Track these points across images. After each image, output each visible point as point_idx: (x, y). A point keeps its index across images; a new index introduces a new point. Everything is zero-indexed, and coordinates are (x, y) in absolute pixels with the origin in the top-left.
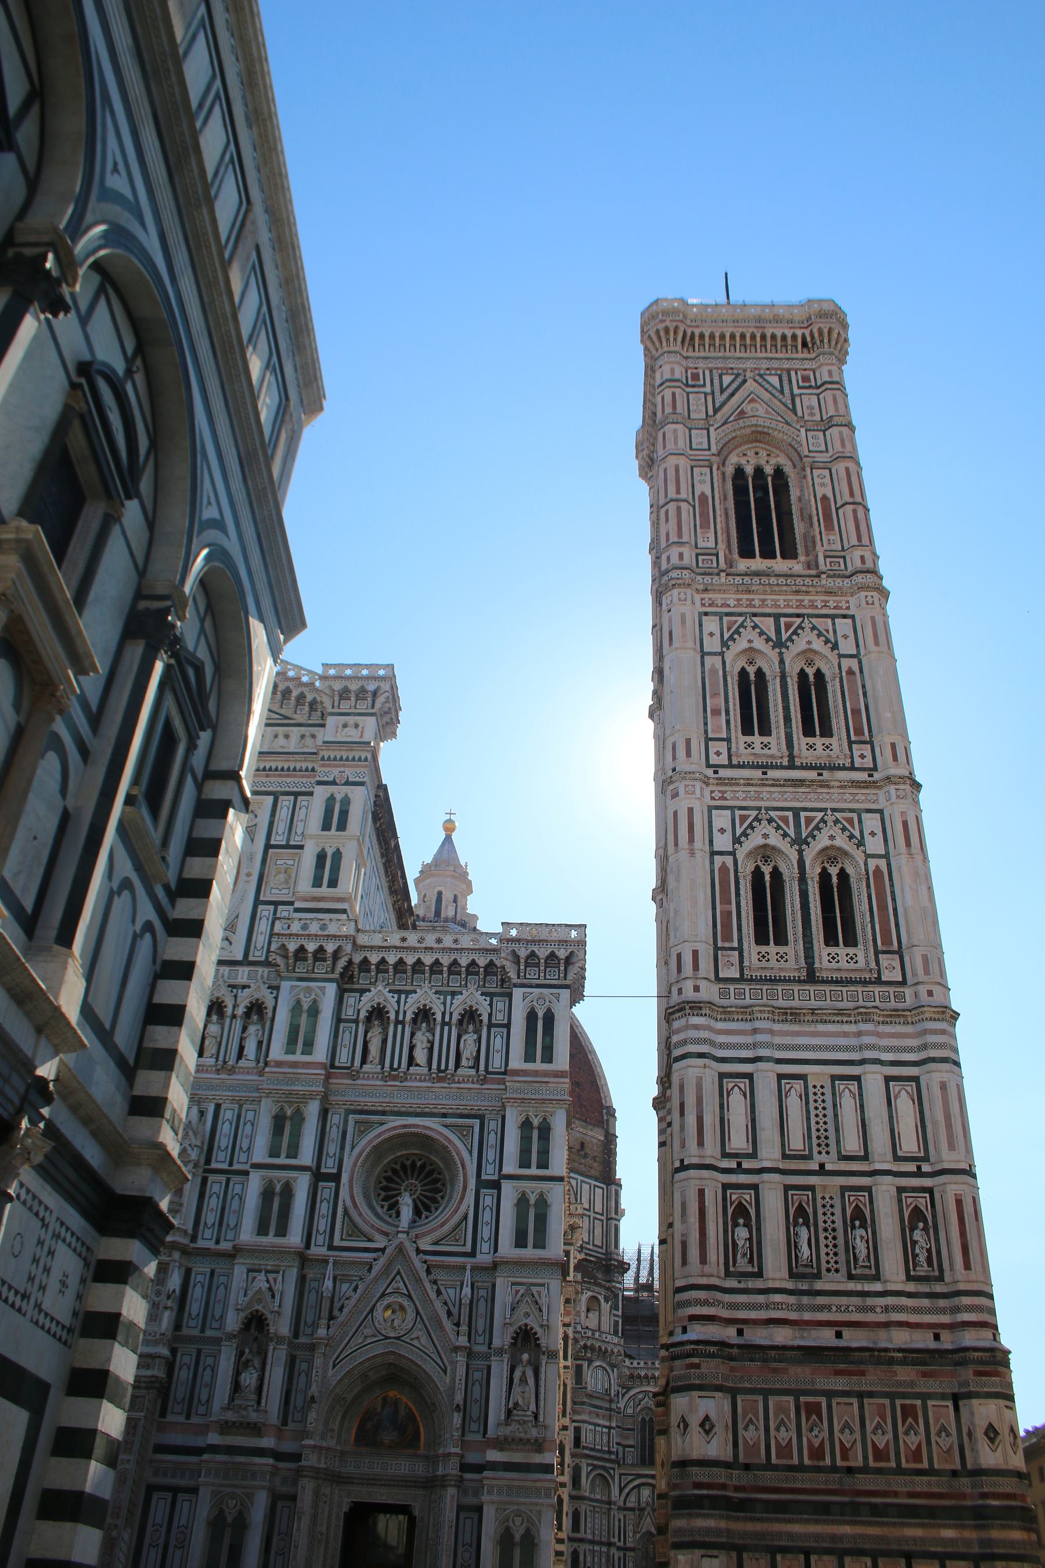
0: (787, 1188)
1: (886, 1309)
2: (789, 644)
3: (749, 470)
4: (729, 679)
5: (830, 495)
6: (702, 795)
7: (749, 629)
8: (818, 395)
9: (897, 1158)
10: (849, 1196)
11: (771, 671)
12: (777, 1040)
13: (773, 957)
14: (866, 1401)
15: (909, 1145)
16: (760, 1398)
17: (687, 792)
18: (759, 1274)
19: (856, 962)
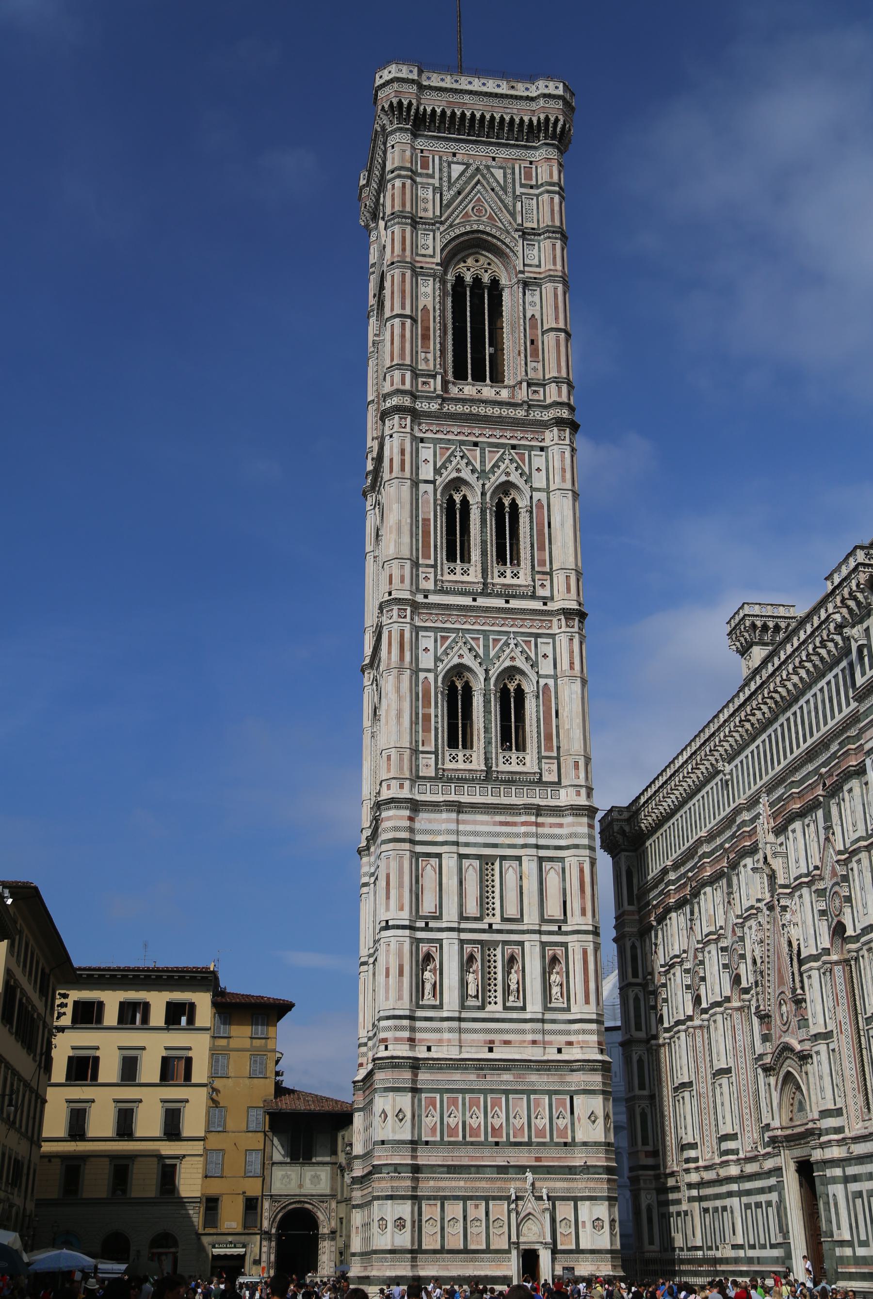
0: (462, 942)
2: (491, 476)
3: (468, 278)
4: (438, 508)
5: (538, 316)
6: (412, 619)
7: (458, 458)
8: (537, 196)
9: (543, 920)
11: (474, 499)
12: (462, 827)
13: (460, 757)
14: (511, 1096)
15: (554, 910)
16: (438, 1096)
17: (400, 616)
18: (440, 1007)
19: (524, 764)
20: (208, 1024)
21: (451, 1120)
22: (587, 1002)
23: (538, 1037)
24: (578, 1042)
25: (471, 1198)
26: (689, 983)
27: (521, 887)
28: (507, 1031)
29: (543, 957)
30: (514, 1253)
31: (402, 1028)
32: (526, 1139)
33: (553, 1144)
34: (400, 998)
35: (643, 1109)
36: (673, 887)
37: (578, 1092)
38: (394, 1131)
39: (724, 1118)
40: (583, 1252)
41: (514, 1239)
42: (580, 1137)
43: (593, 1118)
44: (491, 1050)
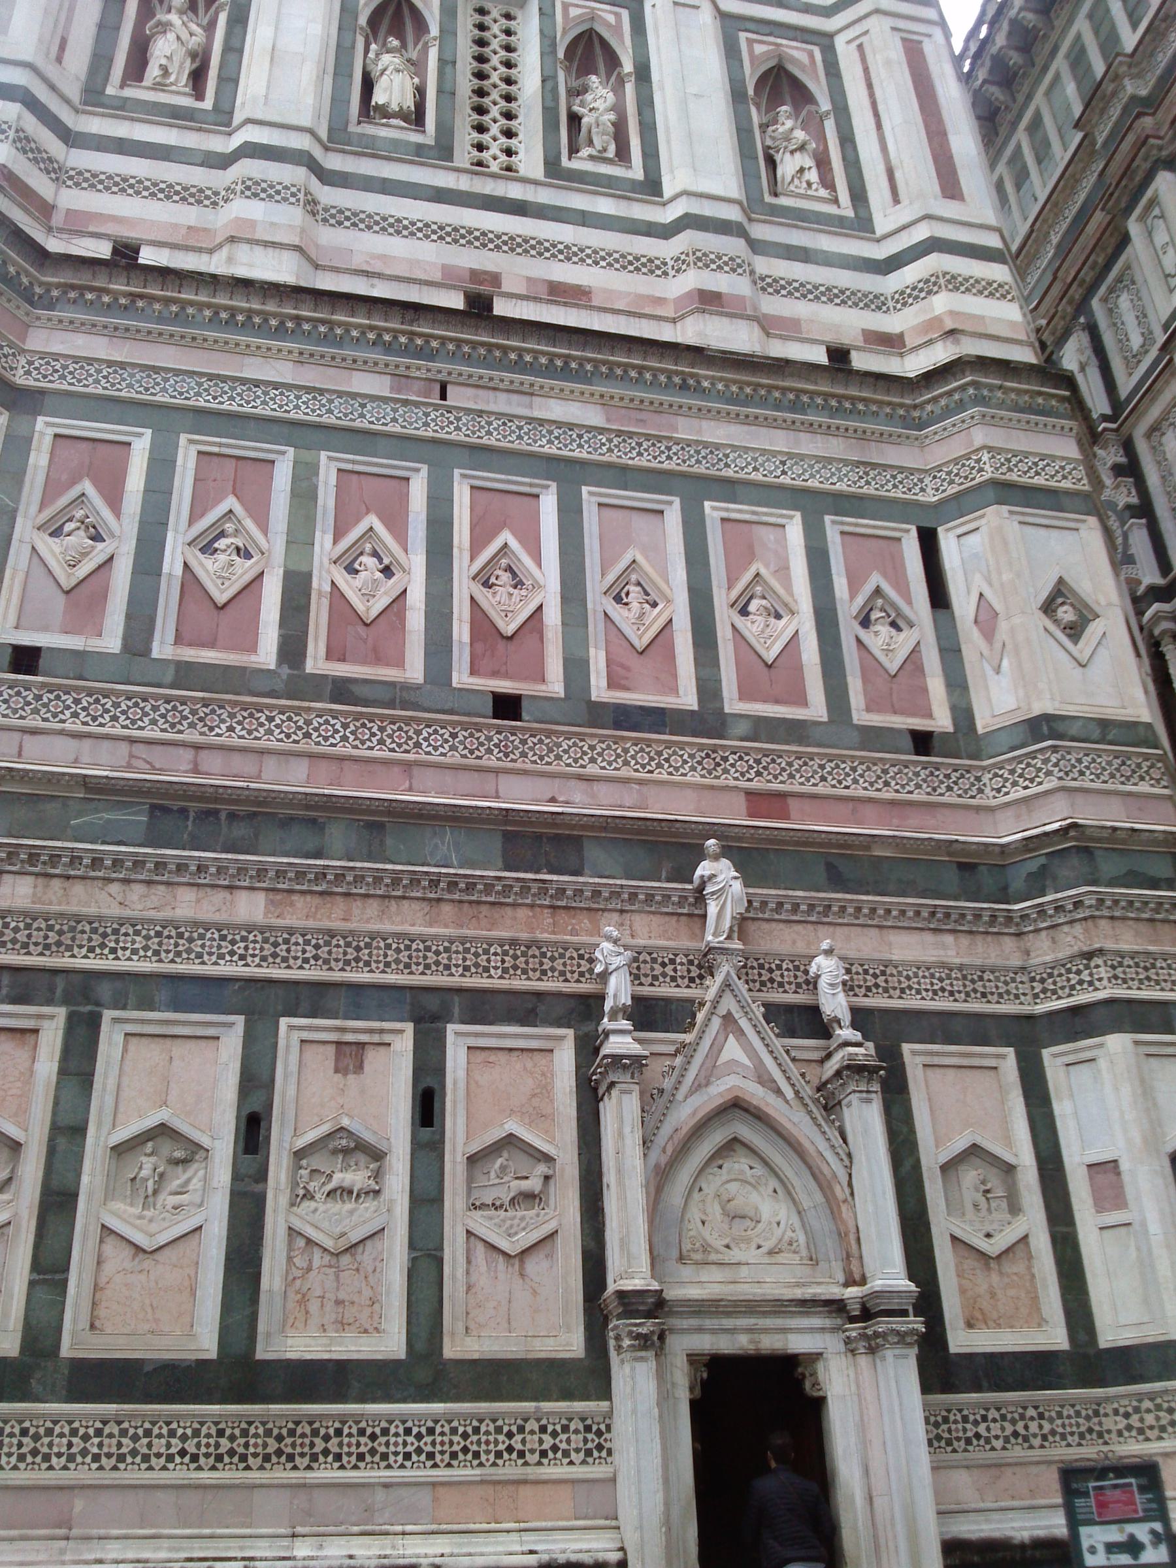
1: (680, 264)
22: (950, 187)
28: (568, 254)
32: (687, 698)
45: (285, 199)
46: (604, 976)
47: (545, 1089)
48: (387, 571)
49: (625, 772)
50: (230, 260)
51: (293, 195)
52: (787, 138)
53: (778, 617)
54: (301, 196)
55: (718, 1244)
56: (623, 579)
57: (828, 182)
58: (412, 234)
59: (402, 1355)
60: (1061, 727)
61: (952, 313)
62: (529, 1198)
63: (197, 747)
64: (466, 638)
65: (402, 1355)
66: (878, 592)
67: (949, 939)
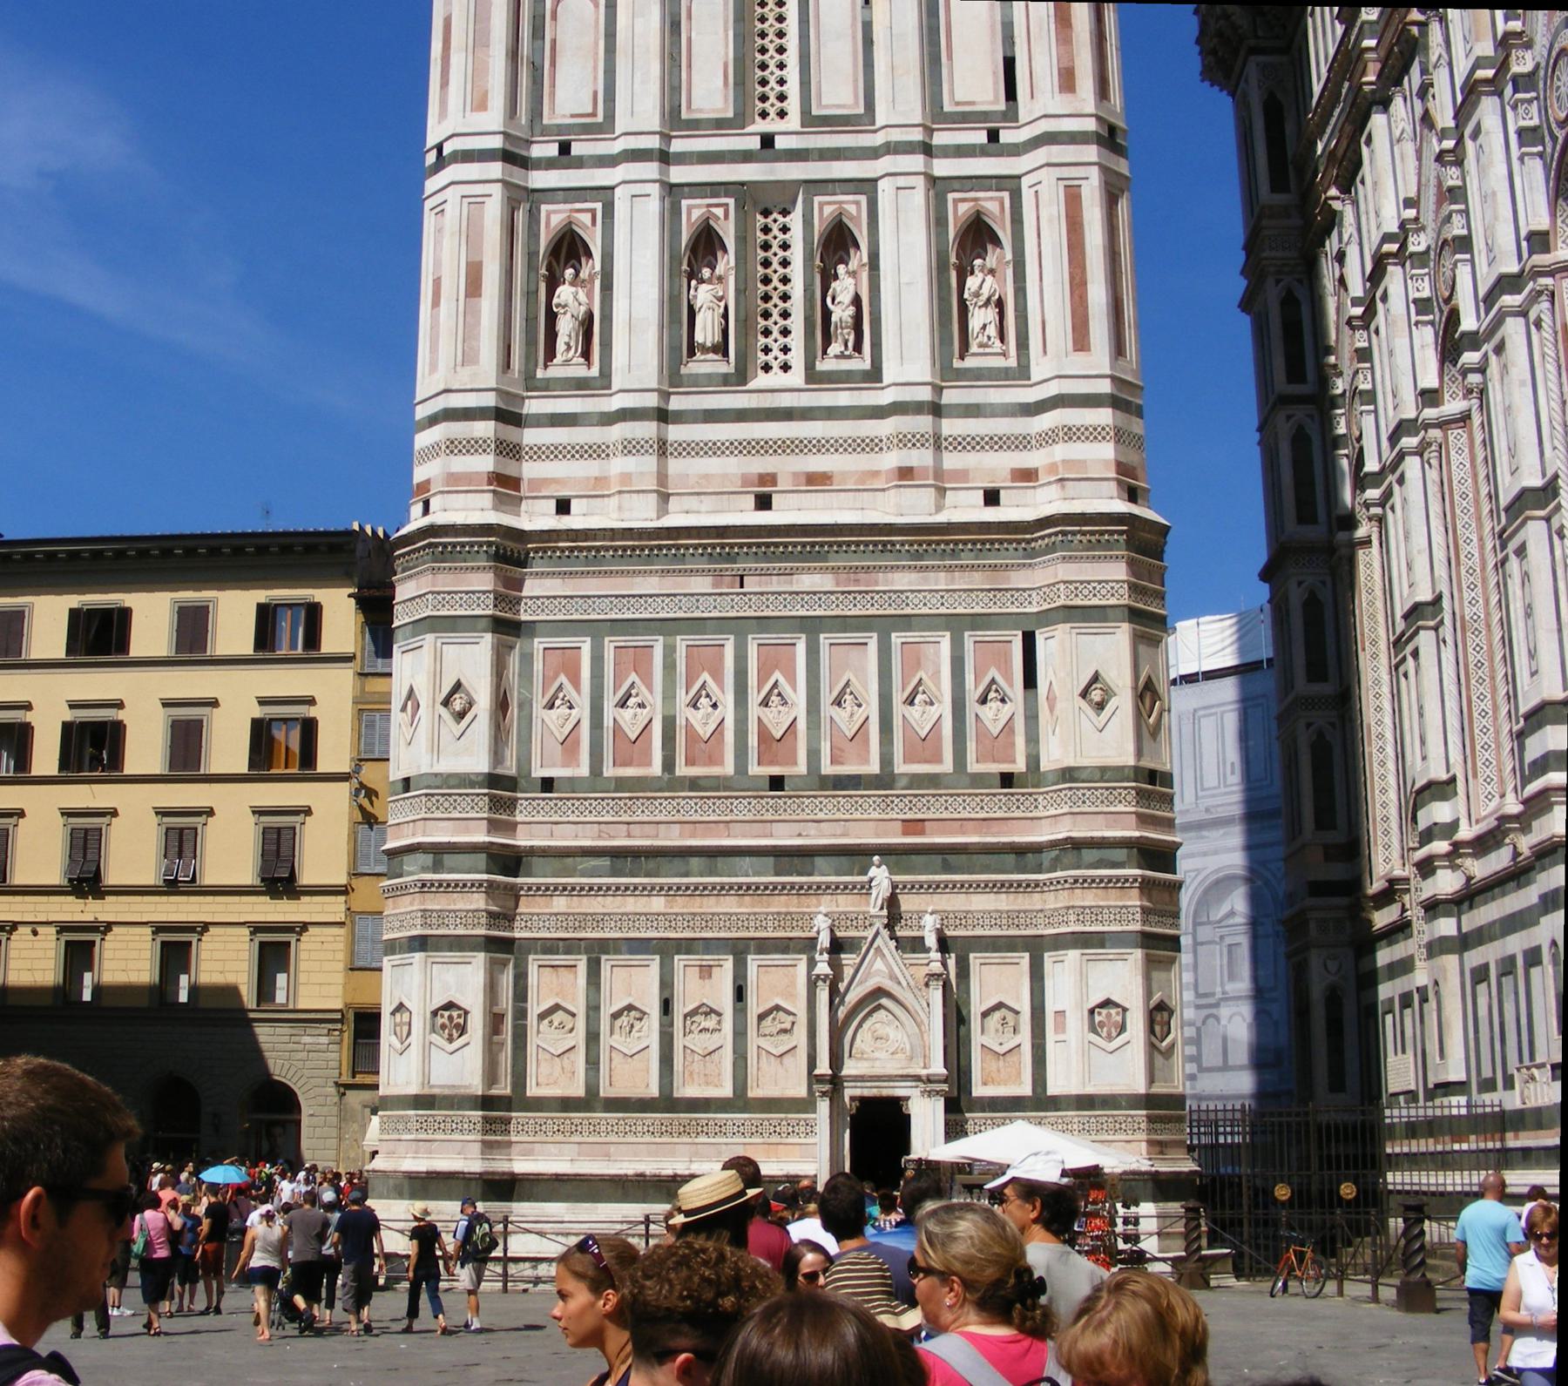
10: (821, 205)
18: (604, 380)
20: (349, 648)
21: (626, 715)
22: (1081, 341)
23: (921, 458)
24: (1053, 468)
25: (686, 946)
26: (1426, 293)
27: (867, 27)
29: (938, 220)
30: (823, 1106)
31: (472, 446)
32: (874, 767)
33: (963, 778)
34: (468, 358)
35: (1320, 734)
36: (1372, 43)
37: (1050, 617)
38: (436, 748)
39: (1532, 655)
40: (1055, 1103)
41: (823, 1068)
42: (1053, 756)
43: (1096, 695)
44: (764, 502)
45: (647, 451)
46: (818, 932)
47: (793, 984)
48: (715, 706)
49: (839, 816)
50: (620, 508)
51: (651, 446)
52: (977, 295)
53: (932, 704)
54: (655, 446)
55: (868, 1050)
56: (842, 692)
57: (1002, 338)
58: (723, 453)
59: (731, 1095)
60: (1076, 775)
61: (1063, 461)
62: (785, 1031)
63: (628, 823)
64: (756, 744)
65: (731, 1095)
66: (993, 681)
67: (1004, 896)
